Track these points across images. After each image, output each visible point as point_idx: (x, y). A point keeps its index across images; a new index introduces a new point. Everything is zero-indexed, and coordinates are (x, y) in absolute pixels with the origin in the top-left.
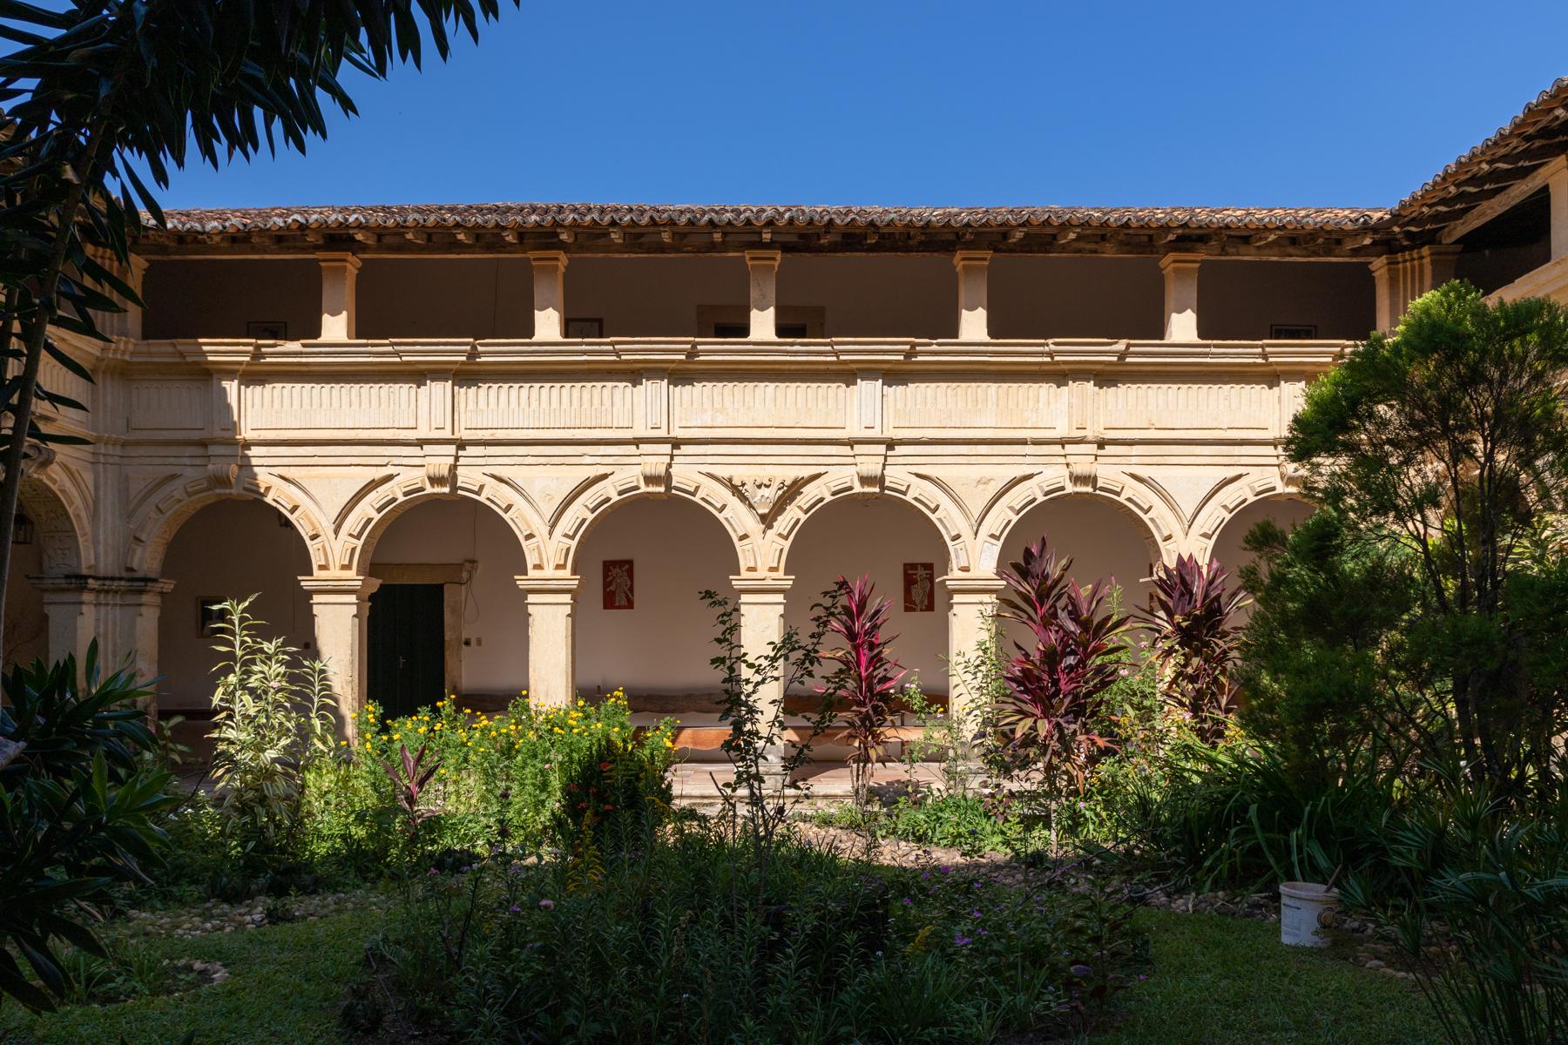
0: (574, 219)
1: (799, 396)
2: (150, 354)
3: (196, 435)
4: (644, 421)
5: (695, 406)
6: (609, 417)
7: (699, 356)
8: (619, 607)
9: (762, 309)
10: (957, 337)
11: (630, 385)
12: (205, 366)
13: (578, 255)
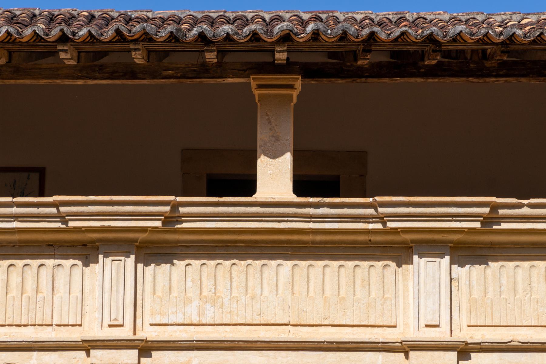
0: (8, 32)
1: (327, 278)
4: (97, 315)
5: (175, 294)
6: (48, 311)
7: (181, 222)
9: (274, 155)
11: (79, 263)
13: (12, 82)
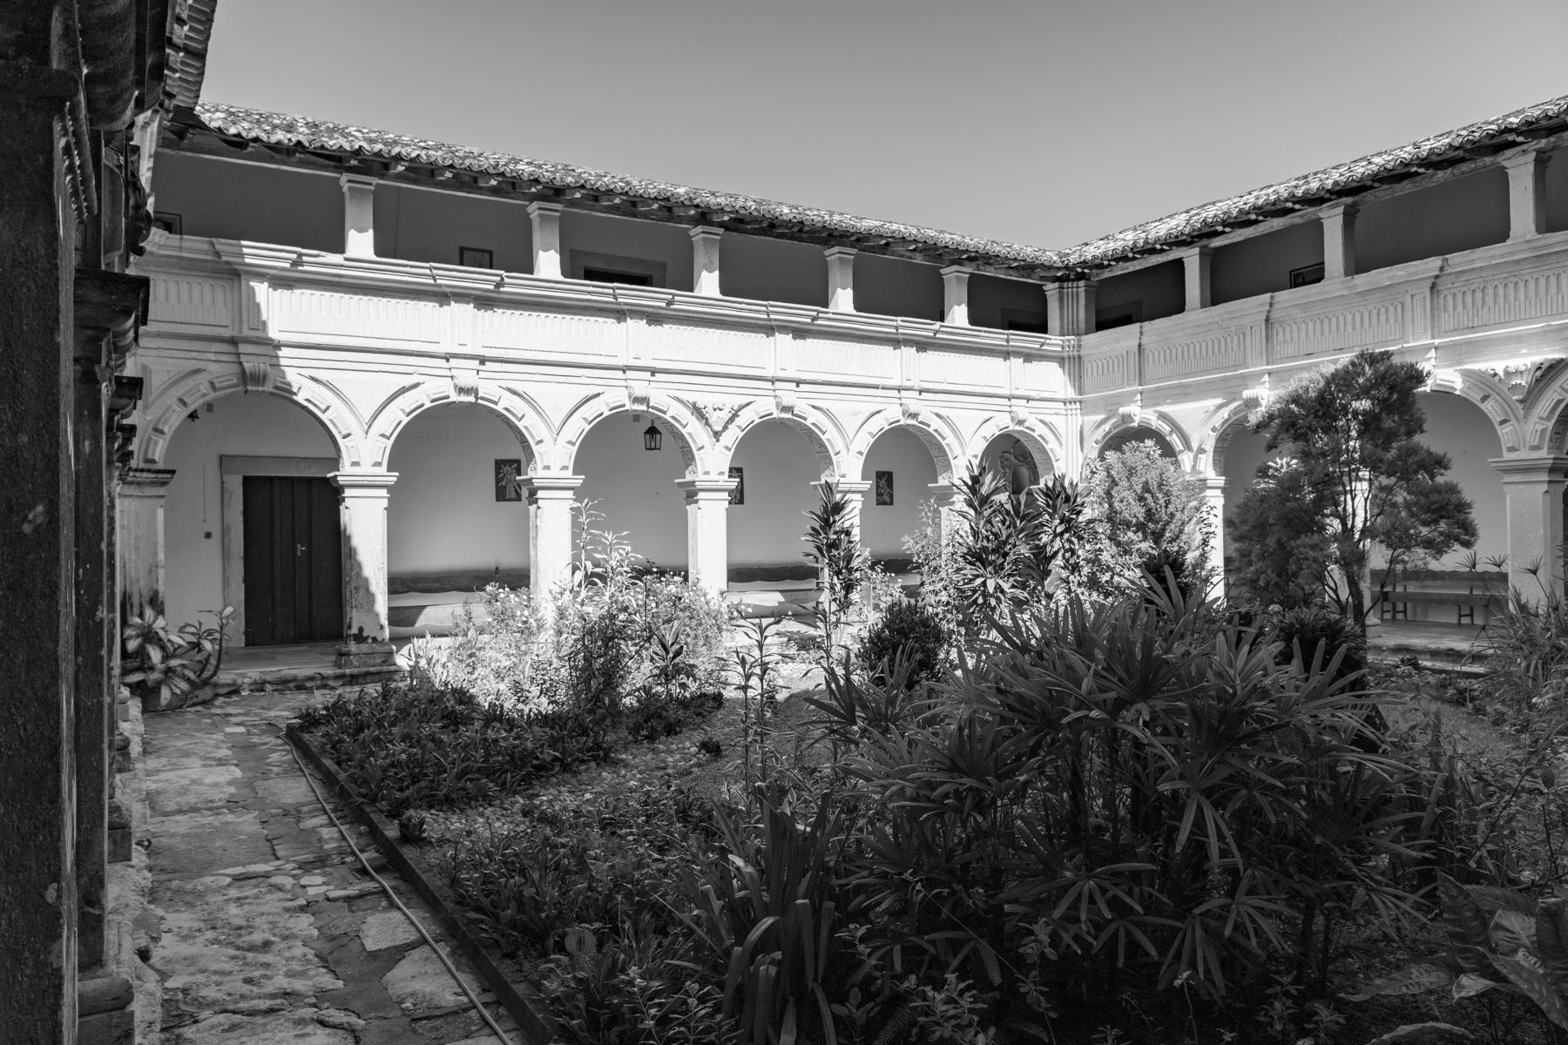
2: (181, 248)
3: (227, 333)
8: (510, 500)
9: (711, 271)
10: (826, 306)
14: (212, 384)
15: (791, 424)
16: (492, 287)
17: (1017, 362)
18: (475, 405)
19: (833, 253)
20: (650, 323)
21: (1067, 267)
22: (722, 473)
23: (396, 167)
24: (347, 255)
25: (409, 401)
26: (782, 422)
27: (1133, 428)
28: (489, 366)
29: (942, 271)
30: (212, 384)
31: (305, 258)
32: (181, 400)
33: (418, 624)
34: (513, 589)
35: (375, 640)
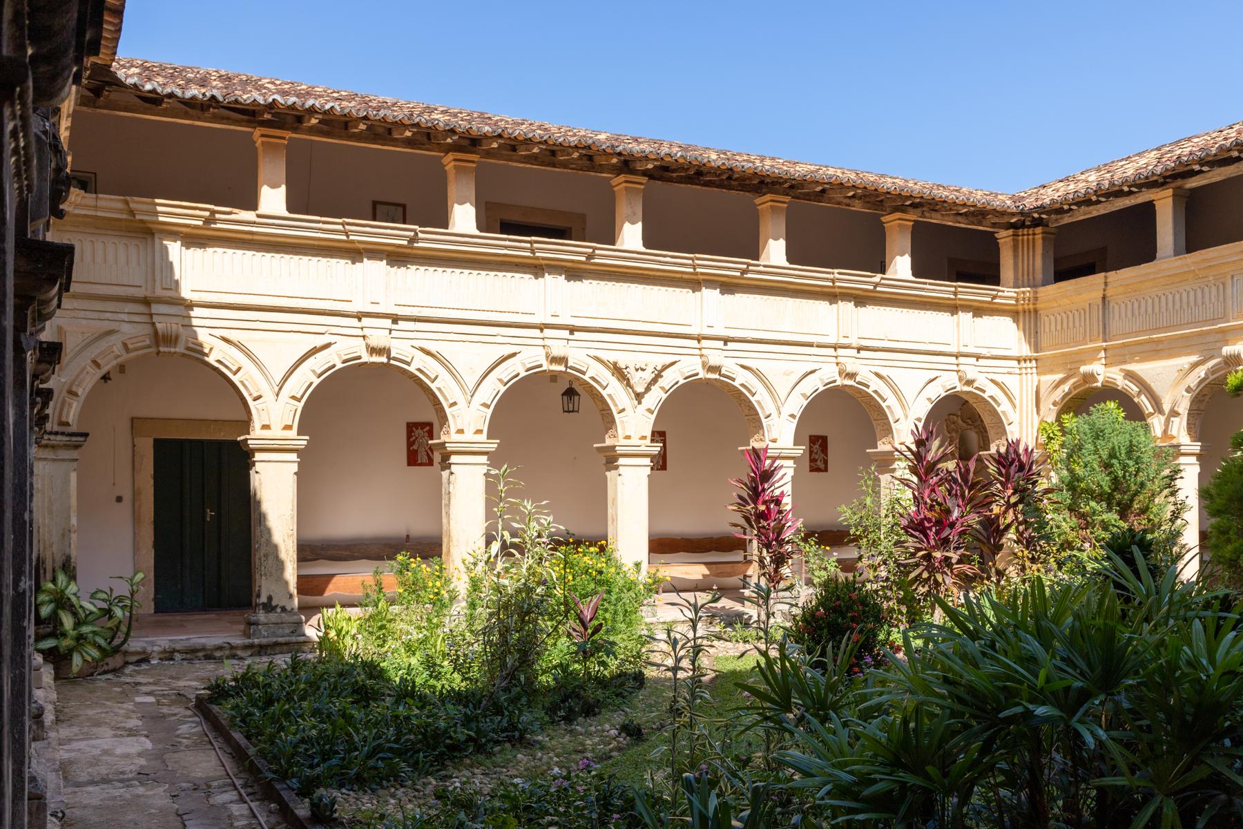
2: (96, 208)
3: (139, 293)
9: (633, 223)
10: (758, 259)
12: (150, 226)
14: (125, 345)
15: (718, 384)
16: (405, 243)
17: (965, 317)
18: (387, 365)
19: (764, 202)
20: (568, 279)
21: (1022, 213)
22: (644, 438)
23: (310, 120)
24: (261, 211)
25: (319, 362)
26: (708, 382)
27: (1096, 388)
28: (402, 325)
29: (883, 219)
30: (125, 345)
31: (217, 216)
32: (95, 362)
33: (327, 594)
34: (424, 558)
35: (284, 609)
